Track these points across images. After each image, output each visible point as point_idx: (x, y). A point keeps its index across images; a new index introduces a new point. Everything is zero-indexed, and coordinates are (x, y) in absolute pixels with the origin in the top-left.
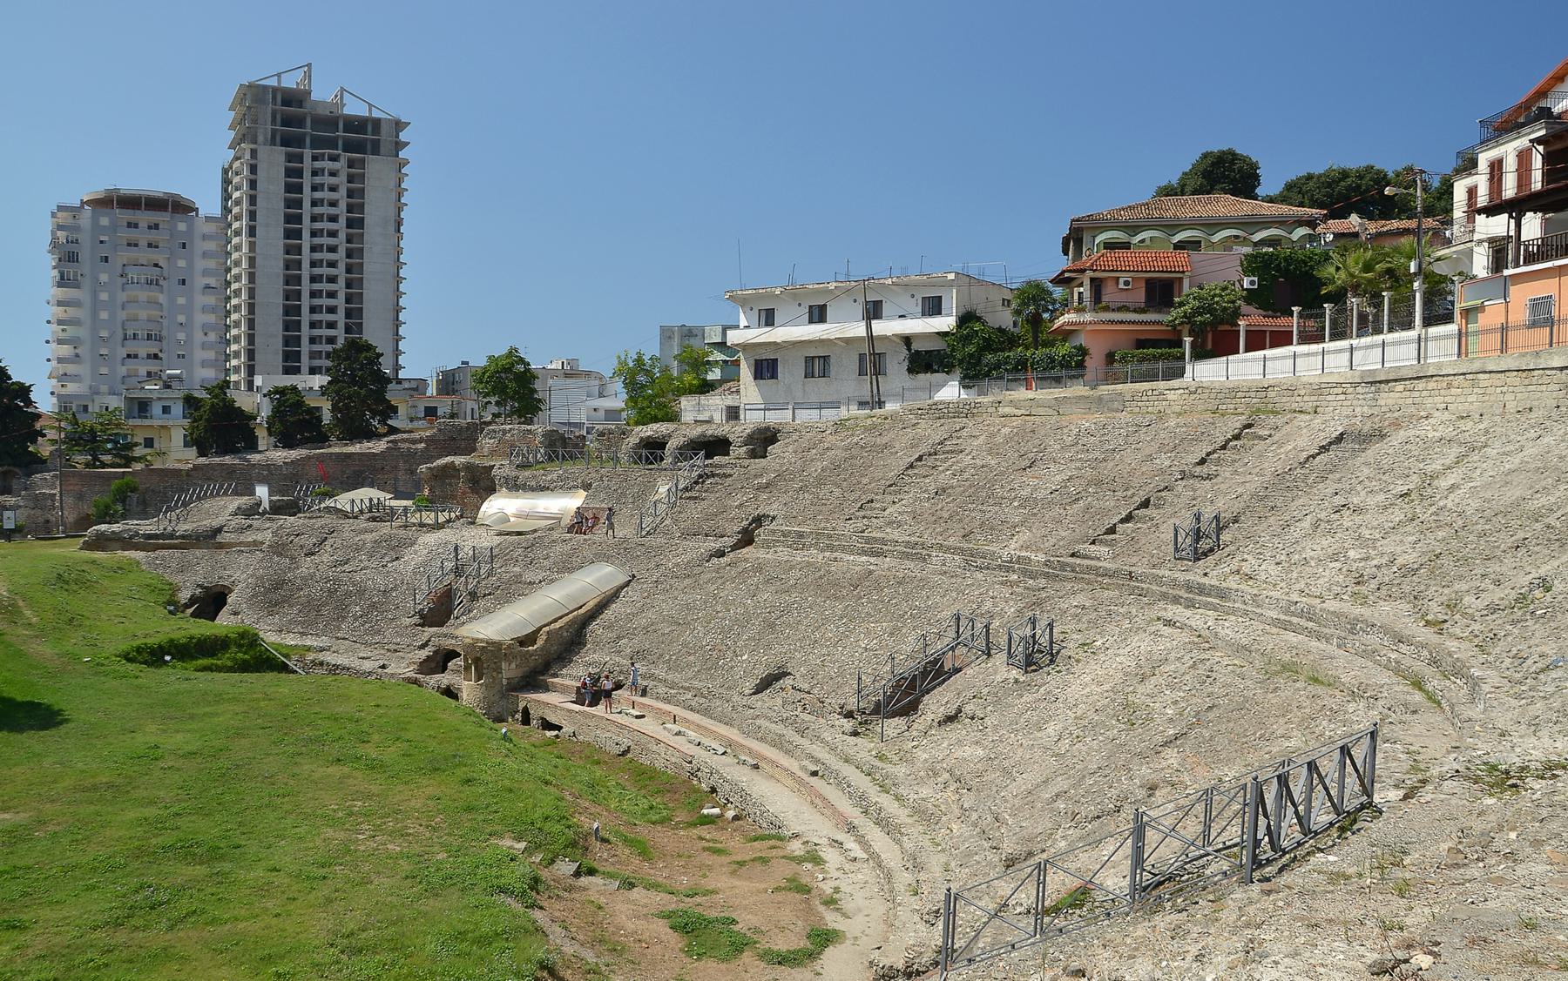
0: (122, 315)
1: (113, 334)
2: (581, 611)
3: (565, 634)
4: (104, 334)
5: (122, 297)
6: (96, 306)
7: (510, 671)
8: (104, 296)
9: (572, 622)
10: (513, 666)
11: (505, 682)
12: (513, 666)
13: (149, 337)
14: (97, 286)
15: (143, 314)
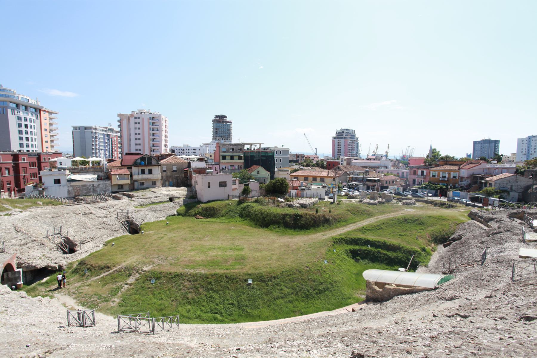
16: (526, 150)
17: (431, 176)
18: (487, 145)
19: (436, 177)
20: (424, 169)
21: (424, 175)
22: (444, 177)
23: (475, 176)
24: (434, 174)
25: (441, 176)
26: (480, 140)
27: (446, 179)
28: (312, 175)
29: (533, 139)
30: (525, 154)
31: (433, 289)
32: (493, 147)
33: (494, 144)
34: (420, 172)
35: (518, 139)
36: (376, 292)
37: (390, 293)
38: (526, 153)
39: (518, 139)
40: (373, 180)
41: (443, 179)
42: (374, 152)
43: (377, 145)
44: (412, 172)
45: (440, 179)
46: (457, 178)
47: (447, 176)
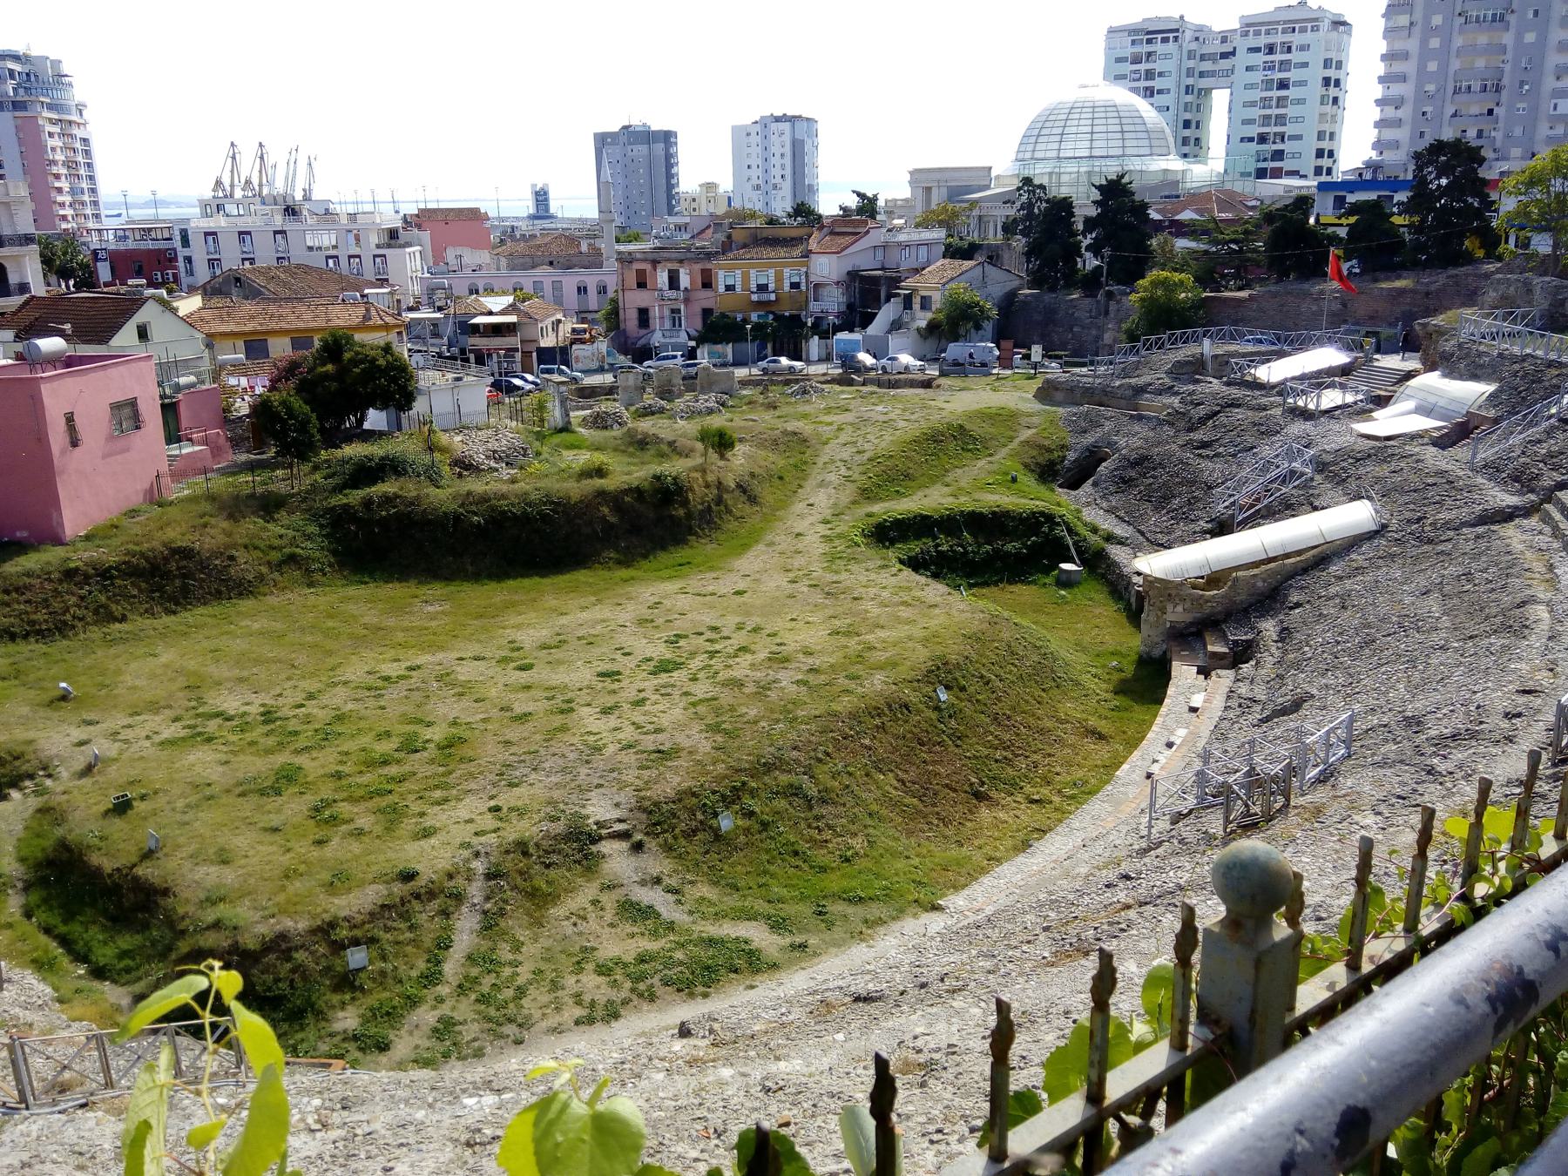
0: (1455, 64)
1: (1441, 89)
2: (1302, 558)
3: (1260, 584)
4: (1431, 88)
5: (1458, 41)
6: (1425, 54)
7: (1177, 614)
8: (1435, 43)
9: (1274, 572)
10: (1180, 609)
11: (1168, 625)
12: (1180, 609)
13: (1484, 89)
14: (1431, 30)
15: (1480, 63)
16: (760, 172)
17: (721, 289)
18: (643, 149)
19: (738, 289)
20: (681, 261)
21: (682, 288)
22: (762, 288)
23: (870, 277)
24: (730, 282)
25: (754, 287)
26: (616, 129)
27: (773, 297)
28: (284, 325)
29: (774, 126)
30: (758, 187)
31: (1377, 532)
32: (663, 160)
33: (662, 145)
34: (662, 278)
35: (734, 129)
36: (1207, 601)
37: (1254, 585)
38: (760, 182)
39: (734, 129)
40: (486, 326)
41: (764, 297)
42: (219, 183)
43: (261, 145)
44: (632, 280)
45: (755, 297)
46: (803, 288)
47: (772, 287)
